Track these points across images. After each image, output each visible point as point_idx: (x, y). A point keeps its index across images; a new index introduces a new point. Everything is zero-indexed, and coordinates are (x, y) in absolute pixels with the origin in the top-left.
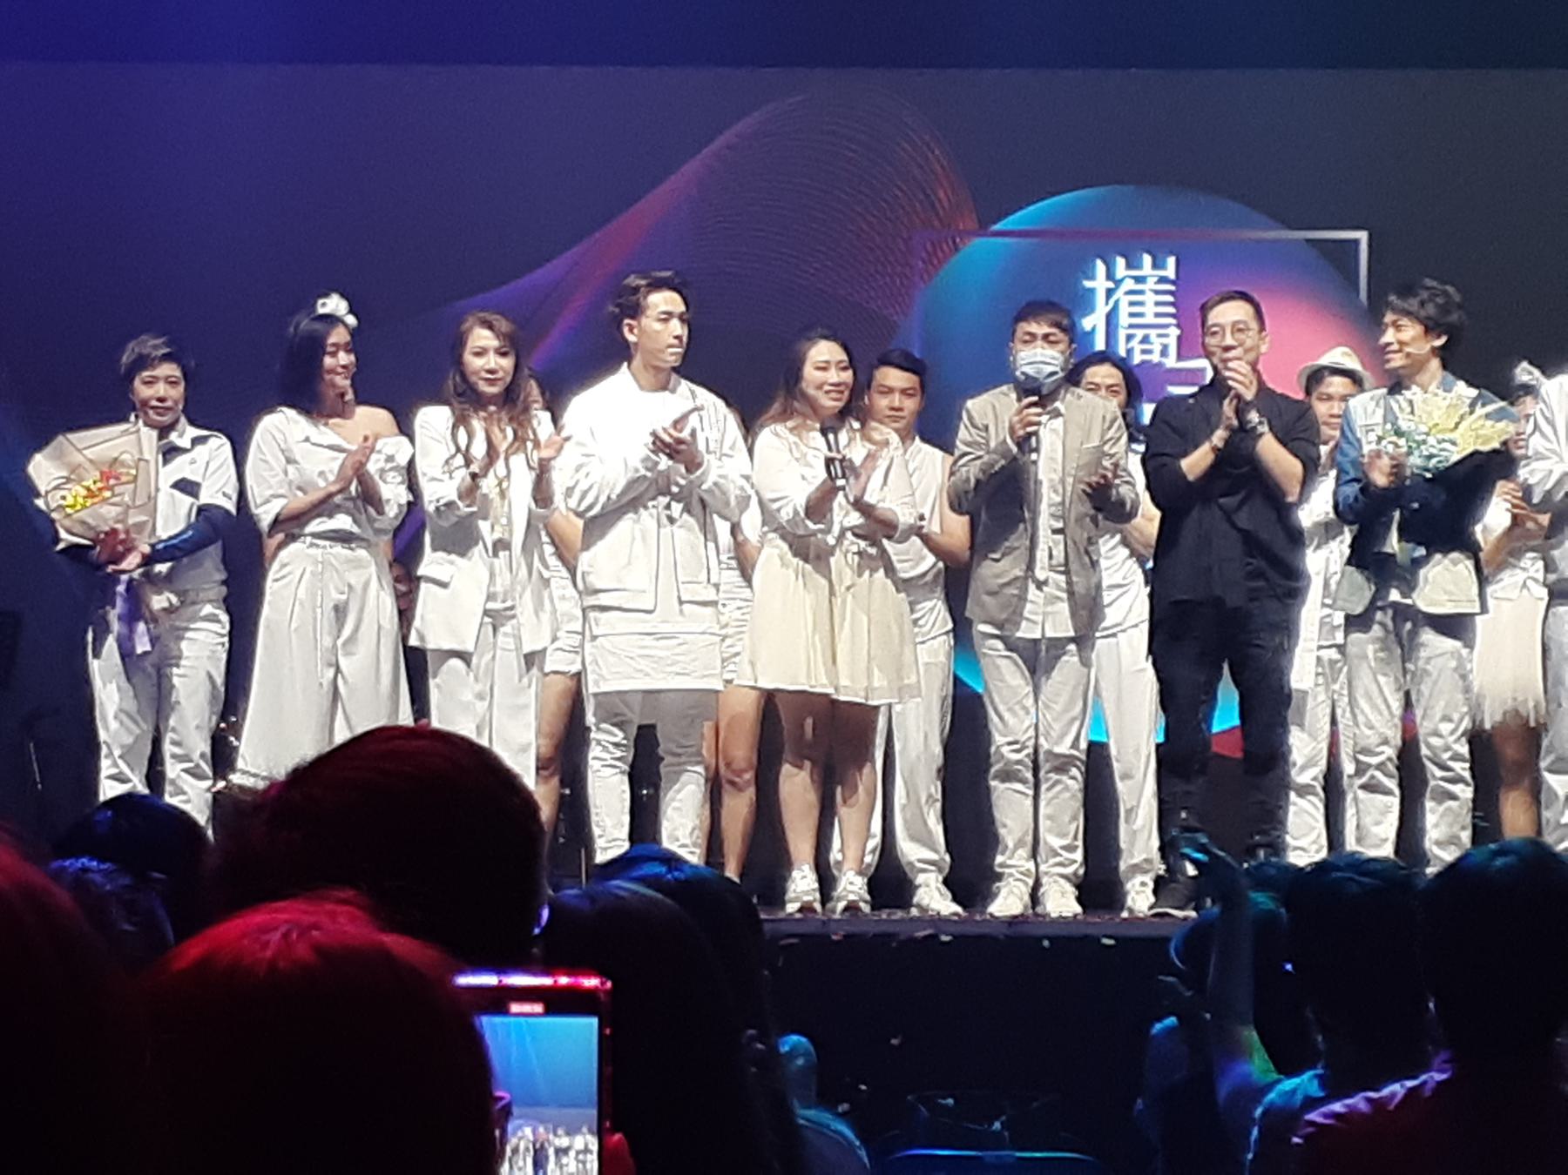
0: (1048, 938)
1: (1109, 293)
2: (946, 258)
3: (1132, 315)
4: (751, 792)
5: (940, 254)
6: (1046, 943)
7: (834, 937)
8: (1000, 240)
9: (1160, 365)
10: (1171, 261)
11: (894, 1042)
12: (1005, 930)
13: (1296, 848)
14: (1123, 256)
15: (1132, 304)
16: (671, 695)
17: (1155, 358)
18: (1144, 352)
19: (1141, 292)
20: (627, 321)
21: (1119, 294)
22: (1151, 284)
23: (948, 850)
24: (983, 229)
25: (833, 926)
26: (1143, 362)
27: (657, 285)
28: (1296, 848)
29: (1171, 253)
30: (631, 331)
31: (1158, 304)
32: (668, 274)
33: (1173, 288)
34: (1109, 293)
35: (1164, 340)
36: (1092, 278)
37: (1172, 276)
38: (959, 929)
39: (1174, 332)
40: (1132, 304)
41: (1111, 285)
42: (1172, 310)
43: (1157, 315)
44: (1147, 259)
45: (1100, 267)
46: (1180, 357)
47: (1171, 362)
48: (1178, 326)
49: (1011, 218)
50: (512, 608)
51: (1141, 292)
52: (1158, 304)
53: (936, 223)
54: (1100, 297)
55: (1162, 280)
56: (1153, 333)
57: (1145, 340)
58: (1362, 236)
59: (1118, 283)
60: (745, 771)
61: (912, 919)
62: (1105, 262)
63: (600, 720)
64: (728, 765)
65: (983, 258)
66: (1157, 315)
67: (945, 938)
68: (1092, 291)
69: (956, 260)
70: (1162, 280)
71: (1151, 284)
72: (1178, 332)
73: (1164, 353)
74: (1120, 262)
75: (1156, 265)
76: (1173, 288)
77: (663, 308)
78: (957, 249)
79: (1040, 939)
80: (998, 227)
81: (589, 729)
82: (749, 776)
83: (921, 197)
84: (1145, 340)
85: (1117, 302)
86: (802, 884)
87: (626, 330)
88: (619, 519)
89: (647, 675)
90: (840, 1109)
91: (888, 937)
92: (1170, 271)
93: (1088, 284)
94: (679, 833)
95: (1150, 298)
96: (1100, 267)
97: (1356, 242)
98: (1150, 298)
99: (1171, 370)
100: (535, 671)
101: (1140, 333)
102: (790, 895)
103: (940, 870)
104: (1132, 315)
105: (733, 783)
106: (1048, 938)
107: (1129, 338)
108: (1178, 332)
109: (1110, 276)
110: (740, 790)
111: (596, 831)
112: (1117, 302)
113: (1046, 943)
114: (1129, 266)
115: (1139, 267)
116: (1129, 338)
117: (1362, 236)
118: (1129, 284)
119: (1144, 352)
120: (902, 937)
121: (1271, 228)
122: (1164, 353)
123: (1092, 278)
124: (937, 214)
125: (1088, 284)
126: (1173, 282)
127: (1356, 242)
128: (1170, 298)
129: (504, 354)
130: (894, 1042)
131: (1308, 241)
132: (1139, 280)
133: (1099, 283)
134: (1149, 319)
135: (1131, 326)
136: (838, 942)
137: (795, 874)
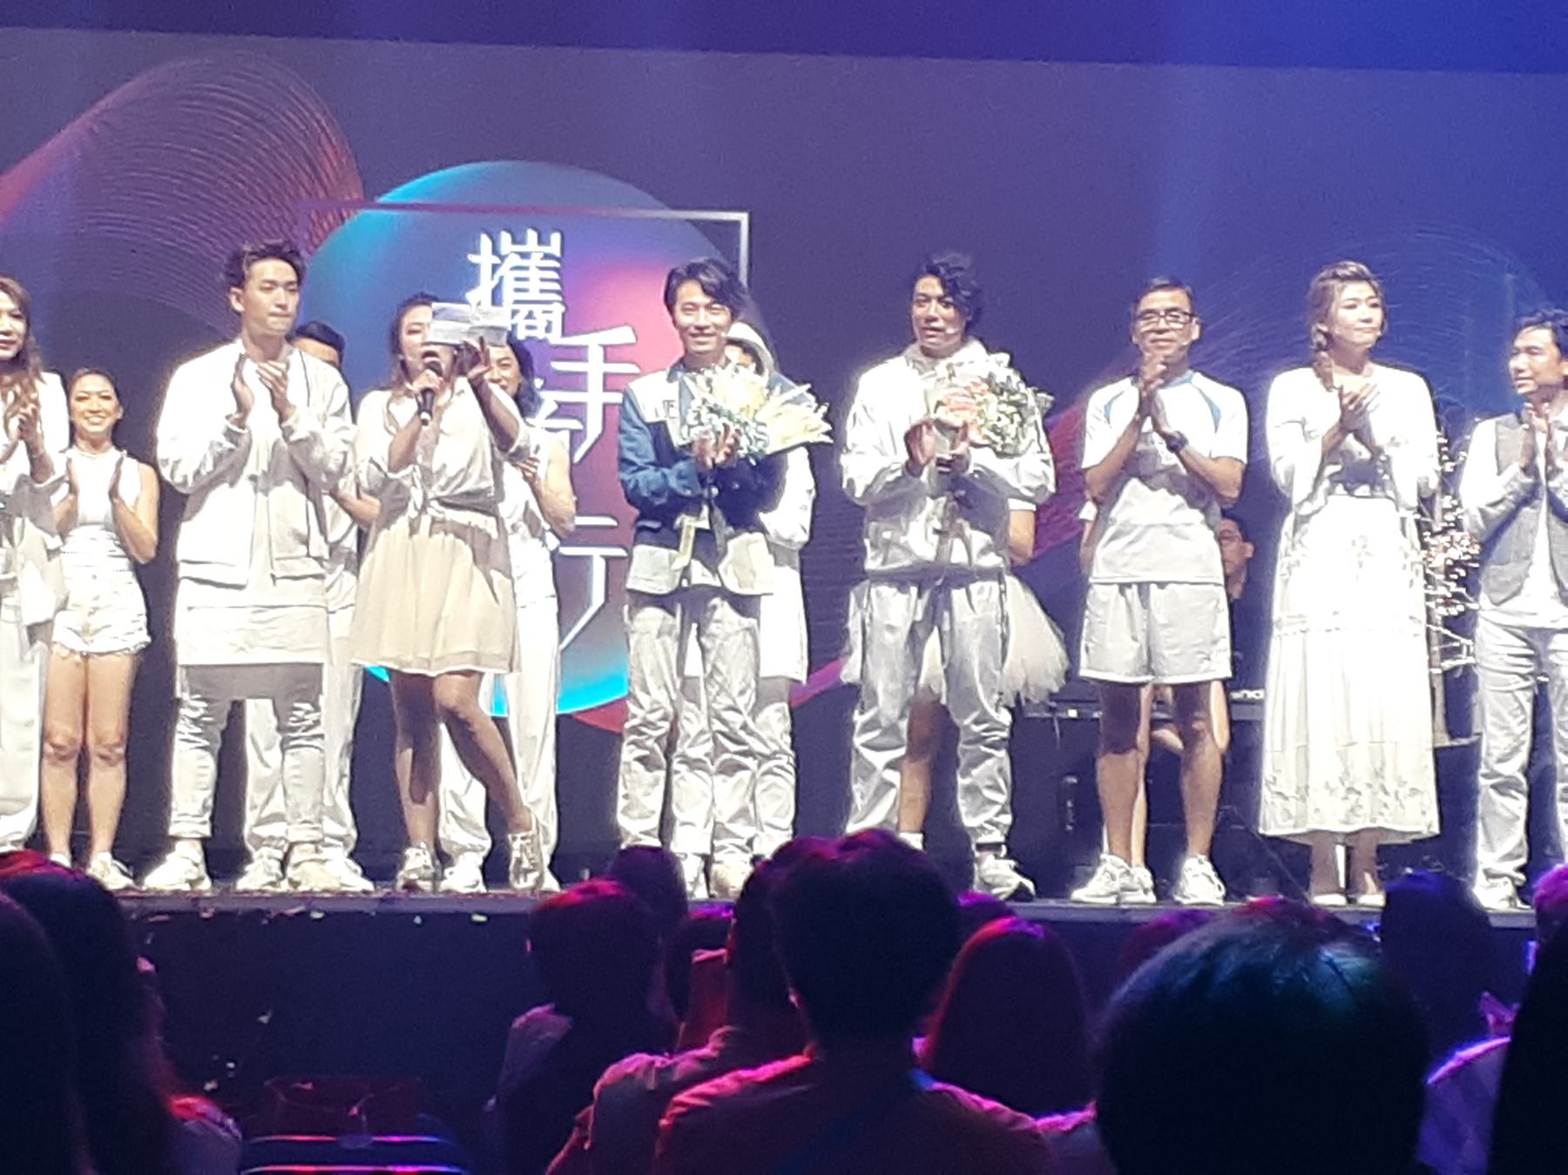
0: (419, 914)
1: (495, 268)
2: (331, 228)
3: (517, 290)
4: (121, 766)
5: (325, 225)
6: (418, 920)
7: (205, 915)
8: (384, 213)
9: (544, 341)
10: (556, 238)
11: (264, 1019)
12: (376, 906)
13: (684, 824)
14: (509, 231)
15: (517, 279)
16: (279, 669)
17: (539, 334)
18: (529, 327)
19: (526, 268)
20: (234, 289)
21: (504, 270)
22: (536, 260)
23: (356, 824)
24: (368, 200)
25: (202, 904)
26: (529, 338)
27: (262, 256)
28: (684, 824)
29: (555, 230)
30: (238, 299)
31: (543, 280)
32: (280, 241)
33: (557, 264)
34: (495, 268)
35: (548, 317)
36: (476, 251)
37: (558, 254)
38: (330, 907)
39: (559, 309)
40: (517, 279)
41: (497, 260)
42: (557, 287)
43: (542, 291)
44: (532, 235)
45: (485, 242)
46: (564, 334)
47: (555, 338)
48: (563, 303)
49: (400, 190)
50: (15, 579)
51: (526, 268)
52: (543, 280)
53: (322, 194)
54: (485, 272)
55: (547, 256)
56: (537, 309)
57: (530, 316)
58: (743, 218)
59: (502, 258)
60: (118, 745)
61: (282, 895)
62: (491, 237)
63: (192, 693)
64: (99, 741)
65: (368, 232)
66: (542, 291)
67: (317, 915)
68: (476, 266)
69: (340, 230)
70: (547, 256)
71: (536, 260)
72: (562, 309)
73: (548, 329)
74: (505, 238)
75: (542, 240)
76: (557, 264)
77: (271, 277)
78: (343, 219)
79: (414, 915)
80: (384, 199)
81: (179, 702)
82: (121, 750)
83: (308, 168)
84: (530, 316)
85: (501, 278)
86: (417, 860)
87: (233, 299)
88: (207, 493)
89: (242, 649)
90: (209, 1086)
91: (260, 913)
92: (555, 246)
93: (472, 258)
94: (301, 810)
95: (535, 275)
96: (485, 242)
97: (737, 224)
98: (535, 275)
99: (557, 347)
100: (39, 644)
101: (524, 309)
102: (401, 873)
103: (346, 846)
104: (517, 290)
105: (103, 757)
106: (419, 914)
107: (514, 313)
108: (562, 309)
109: (495, 251)
110: (113, 765)
111: (174, 805)
112: (501, 278)
113: (418, 920)
114: (514, 242)
115: (523, 242)
116: (514, 313)
117: (743, 218)
118: (514, 260)
119: (529, 327)
120: (273, 914)
121: (655, 208)
122: (548, 329)
123: (476, 251)
124: (322, 185)
125: (472, 258)
126: (558, 259)
127: (737, 224)
128: (555, 275)
129: (17, 317)
130: (264, 1019)
131: (695, 223)
132: (524, 255)
133: (484, 258)
134: (534, 295)
135: (517, 302)
136: (206, 919)
137: (410, 852)
